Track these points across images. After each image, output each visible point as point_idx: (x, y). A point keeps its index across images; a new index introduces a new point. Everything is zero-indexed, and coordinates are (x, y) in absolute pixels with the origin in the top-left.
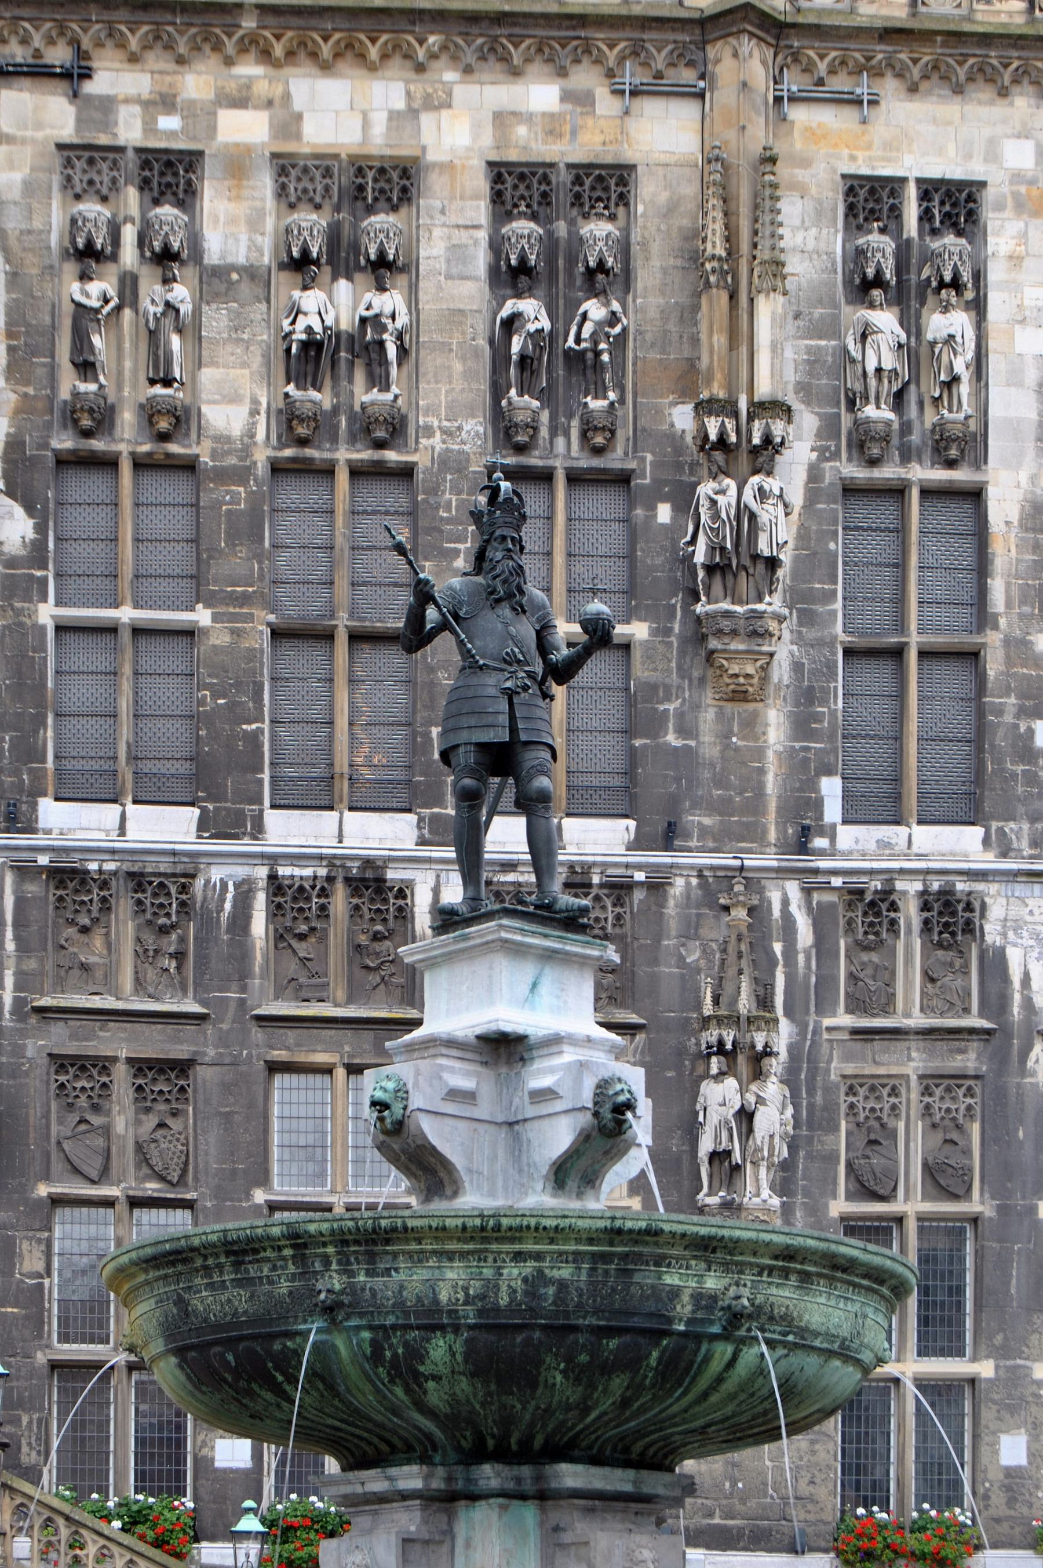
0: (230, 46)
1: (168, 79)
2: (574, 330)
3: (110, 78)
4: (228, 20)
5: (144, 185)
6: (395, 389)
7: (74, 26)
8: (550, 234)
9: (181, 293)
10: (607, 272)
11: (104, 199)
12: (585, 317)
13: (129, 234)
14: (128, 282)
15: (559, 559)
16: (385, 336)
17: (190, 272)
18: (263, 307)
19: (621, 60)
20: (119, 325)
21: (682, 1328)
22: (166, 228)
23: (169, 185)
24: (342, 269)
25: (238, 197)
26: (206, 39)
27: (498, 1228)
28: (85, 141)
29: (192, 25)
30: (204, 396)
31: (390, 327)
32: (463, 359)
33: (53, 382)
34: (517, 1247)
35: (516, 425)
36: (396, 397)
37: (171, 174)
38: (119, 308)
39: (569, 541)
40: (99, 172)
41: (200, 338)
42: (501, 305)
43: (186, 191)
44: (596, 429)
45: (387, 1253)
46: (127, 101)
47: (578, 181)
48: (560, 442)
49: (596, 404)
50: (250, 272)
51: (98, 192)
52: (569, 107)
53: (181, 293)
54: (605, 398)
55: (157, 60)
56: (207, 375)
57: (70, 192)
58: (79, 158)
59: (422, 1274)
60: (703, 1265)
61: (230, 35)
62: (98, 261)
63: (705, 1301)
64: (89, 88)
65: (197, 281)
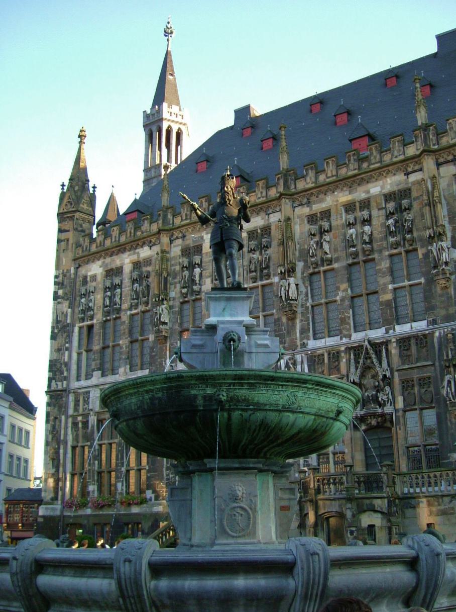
21: (202, 408)
27: (137, 382)
34: (145, 389)
45: (122, 396)
59: (128, 402)
60: (204, 386)
63: (208, 399)
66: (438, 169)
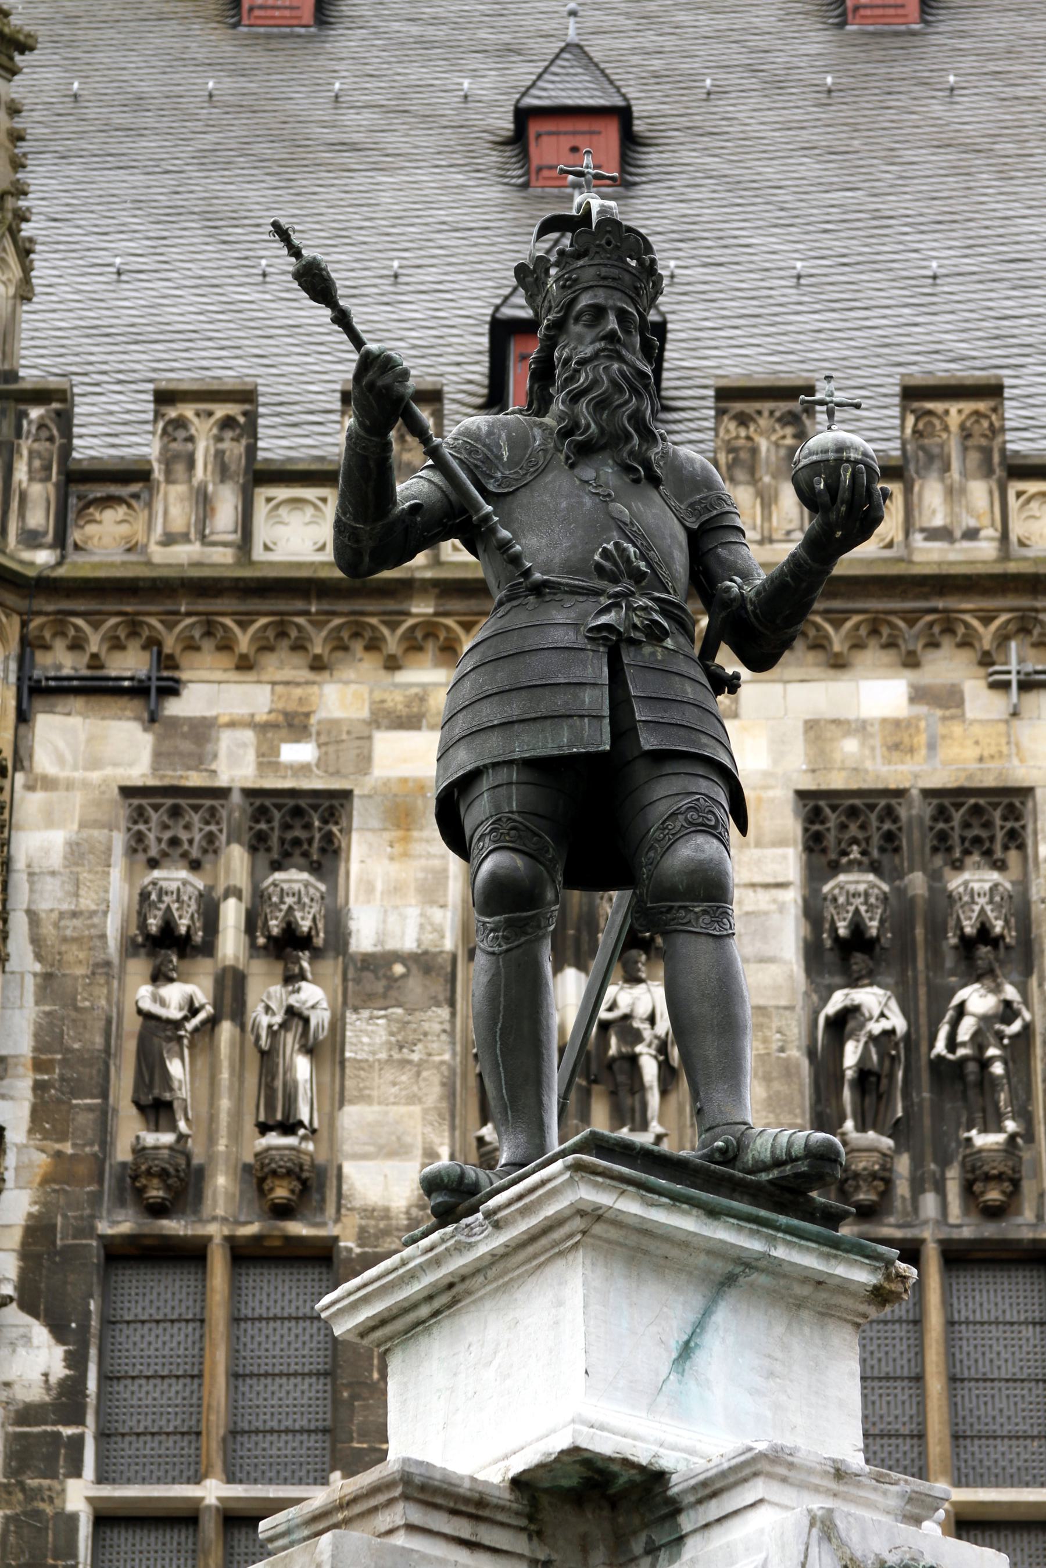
0: (392, 643)
1: (298, 692)
2: (944, 1031)
3: (210, 693)
4: (391, 605)
5: (257, 844)
6: (655, 1127)
7: (153, 621)
8: (900, 892)
9: (311, 995)
10: (995, 942)
11: (195, 866)
12: (961, 1011)
13: (232, 914)
14: (229, 982)
15: (935, 1385)
16: (639, 1049)
17: (330, 967)
18: (444, 1012)
19: (1003, 639)
20: (212, 1047)
22: (289, 900)
23: (297, 842)
24: (570, 953)
25: (406, 855)
26: (356, 635)
28: (166, 782)
29: (334, 614)
30: (347, 1148)
31: (647, 1034)
32: (767, 1079)
33: (104, 1134)
35: (856, 1176)
36: (659, 1138)
37: (301, 826)
38: (213, 1022)
39: (950, 1356)
40: (187, 827)
41: (343, 1062)
42: (825, 1000)
43: (323, 850)
44: (988, 1178)
46: (232, 724)
47: (942, 814)
48: (929, 1202)
49: (984, 1140)
50: (423, 962)
51: (185, 855)
52: (922, 709)
53: (311, 995)
54: (1000, 1129)
55: (284, 665)
56: (353, 1117)
57: (141, 857)
58: (156, 808)
61: (393, 626)
62: (182, 956)
64: (174, 708)
65: (338, 980)
66: (23, 717)
